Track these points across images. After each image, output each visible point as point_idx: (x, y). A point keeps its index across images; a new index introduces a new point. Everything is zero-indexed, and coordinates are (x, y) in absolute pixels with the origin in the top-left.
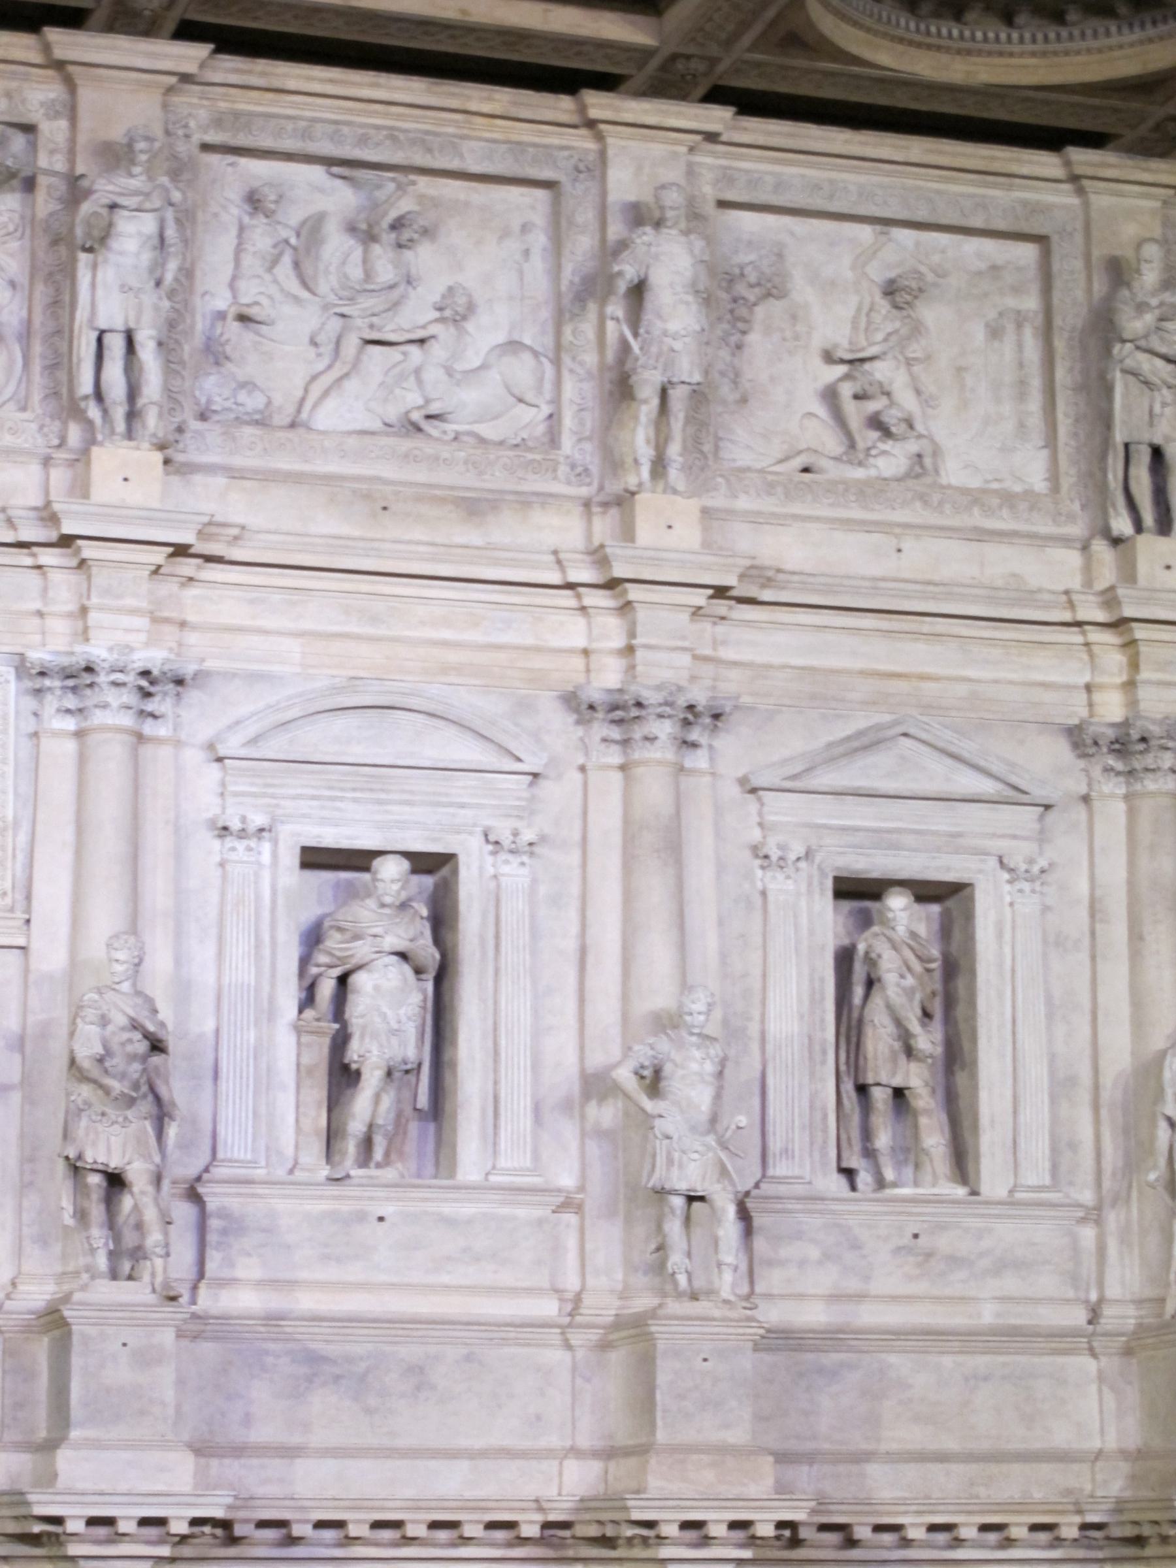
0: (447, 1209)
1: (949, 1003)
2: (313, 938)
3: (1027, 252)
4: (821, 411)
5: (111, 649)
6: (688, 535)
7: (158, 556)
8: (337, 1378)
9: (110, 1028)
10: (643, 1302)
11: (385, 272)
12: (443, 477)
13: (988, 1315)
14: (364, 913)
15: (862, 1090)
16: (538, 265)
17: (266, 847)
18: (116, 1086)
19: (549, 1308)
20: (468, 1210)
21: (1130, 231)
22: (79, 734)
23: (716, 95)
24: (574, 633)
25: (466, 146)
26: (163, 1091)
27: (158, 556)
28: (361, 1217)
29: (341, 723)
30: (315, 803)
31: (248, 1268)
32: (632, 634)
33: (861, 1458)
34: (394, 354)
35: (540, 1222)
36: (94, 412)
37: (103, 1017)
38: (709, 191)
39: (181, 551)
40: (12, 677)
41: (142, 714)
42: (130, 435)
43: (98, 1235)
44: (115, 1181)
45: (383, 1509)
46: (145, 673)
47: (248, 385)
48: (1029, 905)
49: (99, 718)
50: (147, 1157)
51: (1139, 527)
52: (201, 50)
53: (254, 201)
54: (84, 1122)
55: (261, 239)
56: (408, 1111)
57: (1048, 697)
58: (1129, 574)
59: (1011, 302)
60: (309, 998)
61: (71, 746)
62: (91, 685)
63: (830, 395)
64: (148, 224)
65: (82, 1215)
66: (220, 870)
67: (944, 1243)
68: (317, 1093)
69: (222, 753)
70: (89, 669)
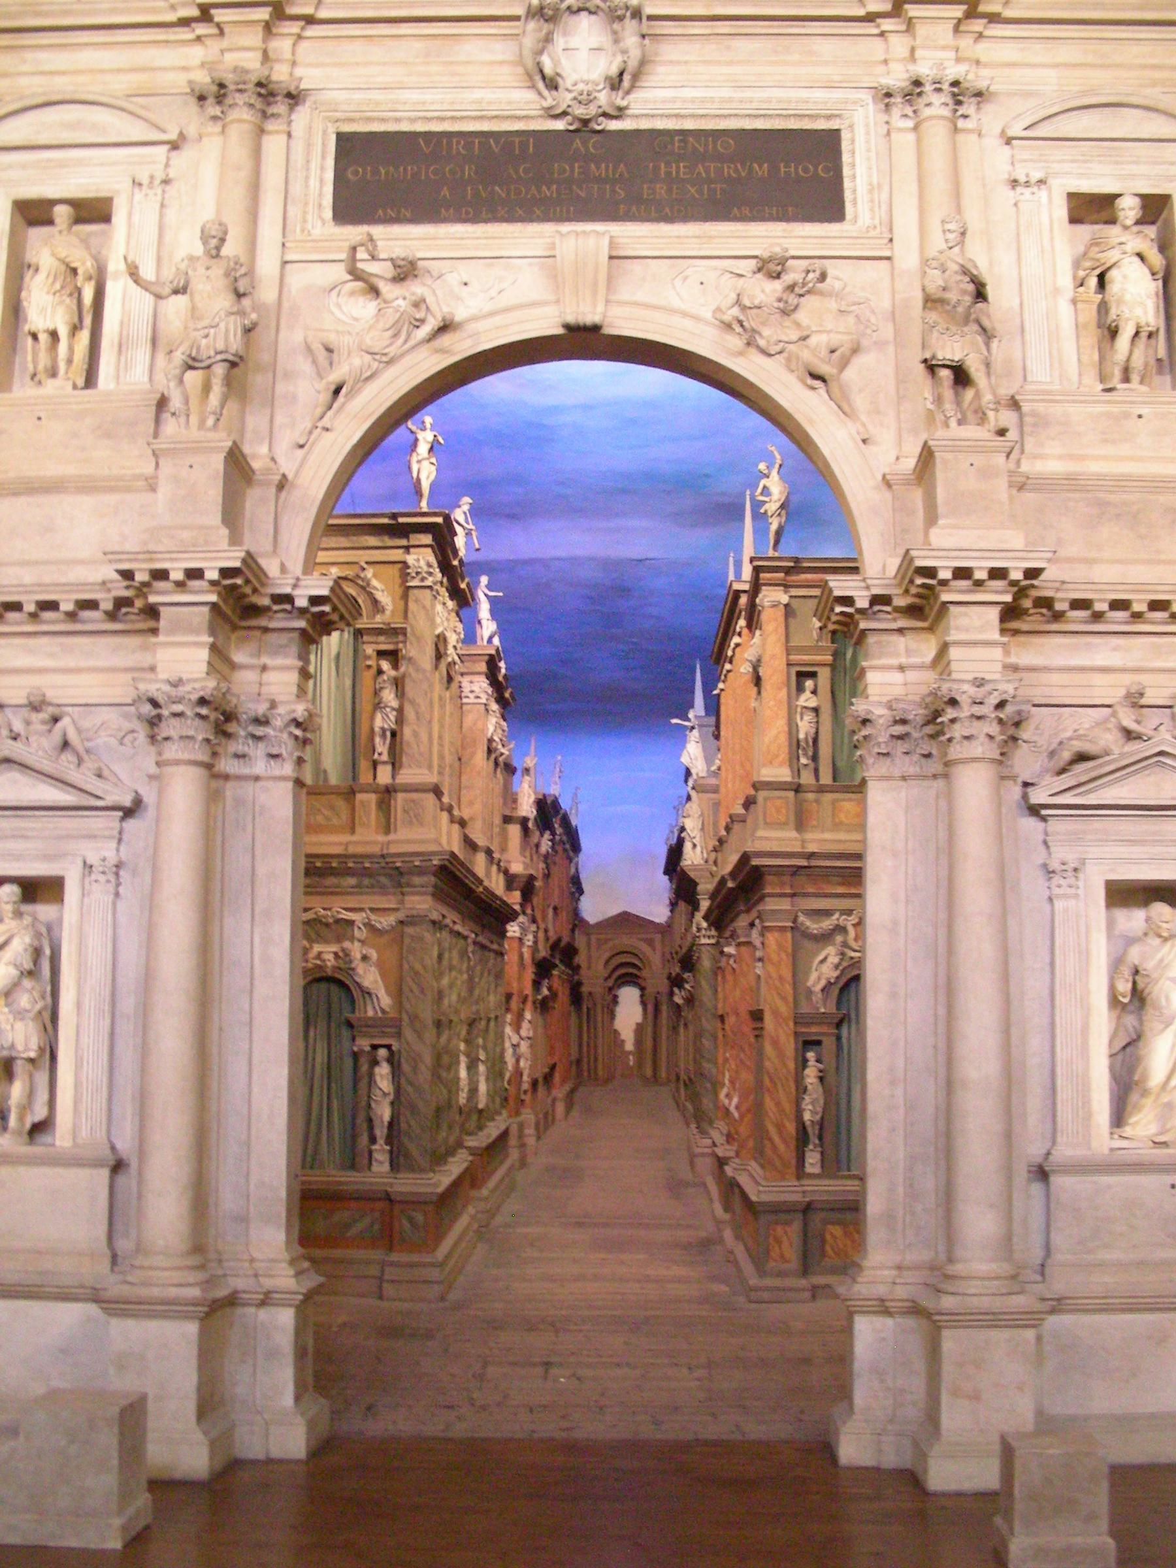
5: (931, 68)
8: (1118, 516)
9: (948, 273)
17: (1043, 194)
22: (916, 128)
26: (986, 323)
28: (1127, 415)
30: (1074, 165)
31: (1053, 448)
37: (942, 265)
40: (870, 101)
43: (949, 406)
45: (1157, 592)
46: (955, 84)
49: (927, 112)
50: (979, 352)
54: (935, 334)
56: (1152, 362)
61: (911, 137)
62: (920, 94)
65: (939, 400)
66: (1014, 209)
68: (1091, 337)
69: (1010, 133)
70: (917, 83)
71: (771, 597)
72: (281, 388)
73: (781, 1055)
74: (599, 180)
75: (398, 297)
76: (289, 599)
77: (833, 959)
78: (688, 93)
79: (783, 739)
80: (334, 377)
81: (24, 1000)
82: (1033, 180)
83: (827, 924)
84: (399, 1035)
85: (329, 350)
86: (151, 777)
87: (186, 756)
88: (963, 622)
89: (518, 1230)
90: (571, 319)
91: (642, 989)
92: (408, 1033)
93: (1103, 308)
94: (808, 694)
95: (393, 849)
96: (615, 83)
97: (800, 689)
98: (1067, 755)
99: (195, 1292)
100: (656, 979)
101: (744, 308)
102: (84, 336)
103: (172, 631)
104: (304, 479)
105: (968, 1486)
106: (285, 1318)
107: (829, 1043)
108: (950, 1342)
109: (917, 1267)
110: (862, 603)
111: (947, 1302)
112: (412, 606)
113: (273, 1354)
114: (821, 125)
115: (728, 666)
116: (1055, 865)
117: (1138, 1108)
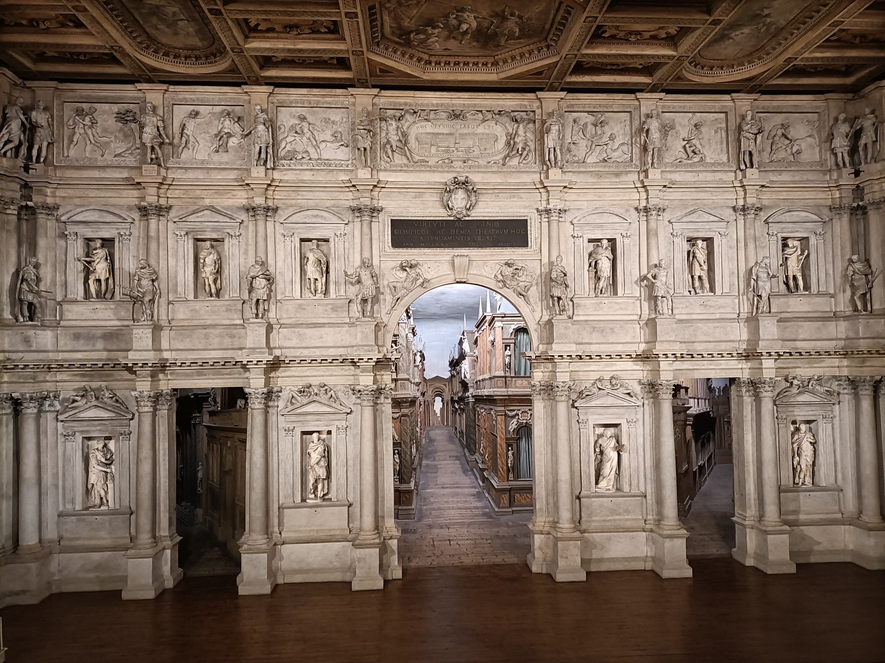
0: (616, 301)
1: (708, 259)
2: (590, 255)
3: (724, 115)
4: (683, 150)
6: (658, 176)
7: (561, 188)
10: (653, 316)
11: (599, 132)
12: (612, 169)
13: (718, 316)
14: (600, 250)
15: (692, 277)
16: (628, 128)
18: (559, 282)
19: (636, 318)
20: (619, 301)
21: (744, 109)
23: (662, 91)
24: (637, 196)
25: (614, 106)
27: (561, 188)
28: (601, 303)
29: (594, 215)
32: (648, 196)
33: (694, 342)
34: (601, 147)
35: (633, 303)
36: (548, 163)
38: (660, 110)
39: (565, 187)
41: (559, 217)
42: (555, 167)
43: (557, 308)
44: (559, 298)
47: (575, 156)
48: (724, 241)
49: (552, 218)
51: (746, 168)
52: (565, 93)
53: (575, 121)
55: (576, 128)
57: (728, 201)
58: (744, 176)
59: (720, 126)
60: (590, 265)
63: (684, 147)
64: (557, 127)
65: (553, 305)
67: (709, 303)
68: (593, 282)
71: (498, 324)
72: (382, 297)
73: (502, 449)
74: (462, 235)
75: (413, 273)
76: (390, 359)
77: (516, 423)
78: (487, 210)
79: (502, 364)
80: (397, 297)
81: (322, 463)
82: (579, 235)
83: (514, 413)
84: (401, 447)
85: (395, 287)
86: (354, 404)
87: (369, 404)
88: (560, 366)
89: (428, 491)
90: (458, 280)
91: (443, 399)
92: (403, 446)
93: (596, 273)
94: (507, 351)
95: (398, 397)
96: (468, 209)
97: (506, 349)
98: (584, 395)
99: (377, 541)
100: (447, 397)
101: (502, 276)
102: (324, 278)
103: (362, 372)
104: (390, 324)
105: (565, 580)
106: (395, 542)
107: (515, 445)
108: (560, 544)
109: (549, 522)
110: (533, 357)
111: (559, 535)
112: (400, 328)
113: (393, 551)
114: (523, 218)
115: (480, 332)
116: (580, 421)
117: (602, 481)
